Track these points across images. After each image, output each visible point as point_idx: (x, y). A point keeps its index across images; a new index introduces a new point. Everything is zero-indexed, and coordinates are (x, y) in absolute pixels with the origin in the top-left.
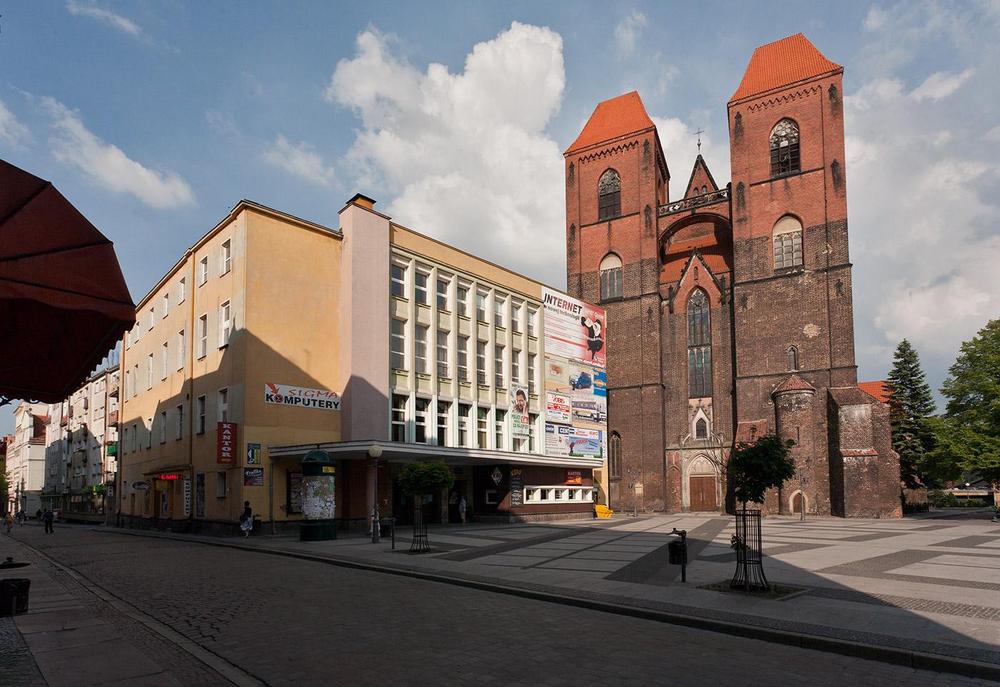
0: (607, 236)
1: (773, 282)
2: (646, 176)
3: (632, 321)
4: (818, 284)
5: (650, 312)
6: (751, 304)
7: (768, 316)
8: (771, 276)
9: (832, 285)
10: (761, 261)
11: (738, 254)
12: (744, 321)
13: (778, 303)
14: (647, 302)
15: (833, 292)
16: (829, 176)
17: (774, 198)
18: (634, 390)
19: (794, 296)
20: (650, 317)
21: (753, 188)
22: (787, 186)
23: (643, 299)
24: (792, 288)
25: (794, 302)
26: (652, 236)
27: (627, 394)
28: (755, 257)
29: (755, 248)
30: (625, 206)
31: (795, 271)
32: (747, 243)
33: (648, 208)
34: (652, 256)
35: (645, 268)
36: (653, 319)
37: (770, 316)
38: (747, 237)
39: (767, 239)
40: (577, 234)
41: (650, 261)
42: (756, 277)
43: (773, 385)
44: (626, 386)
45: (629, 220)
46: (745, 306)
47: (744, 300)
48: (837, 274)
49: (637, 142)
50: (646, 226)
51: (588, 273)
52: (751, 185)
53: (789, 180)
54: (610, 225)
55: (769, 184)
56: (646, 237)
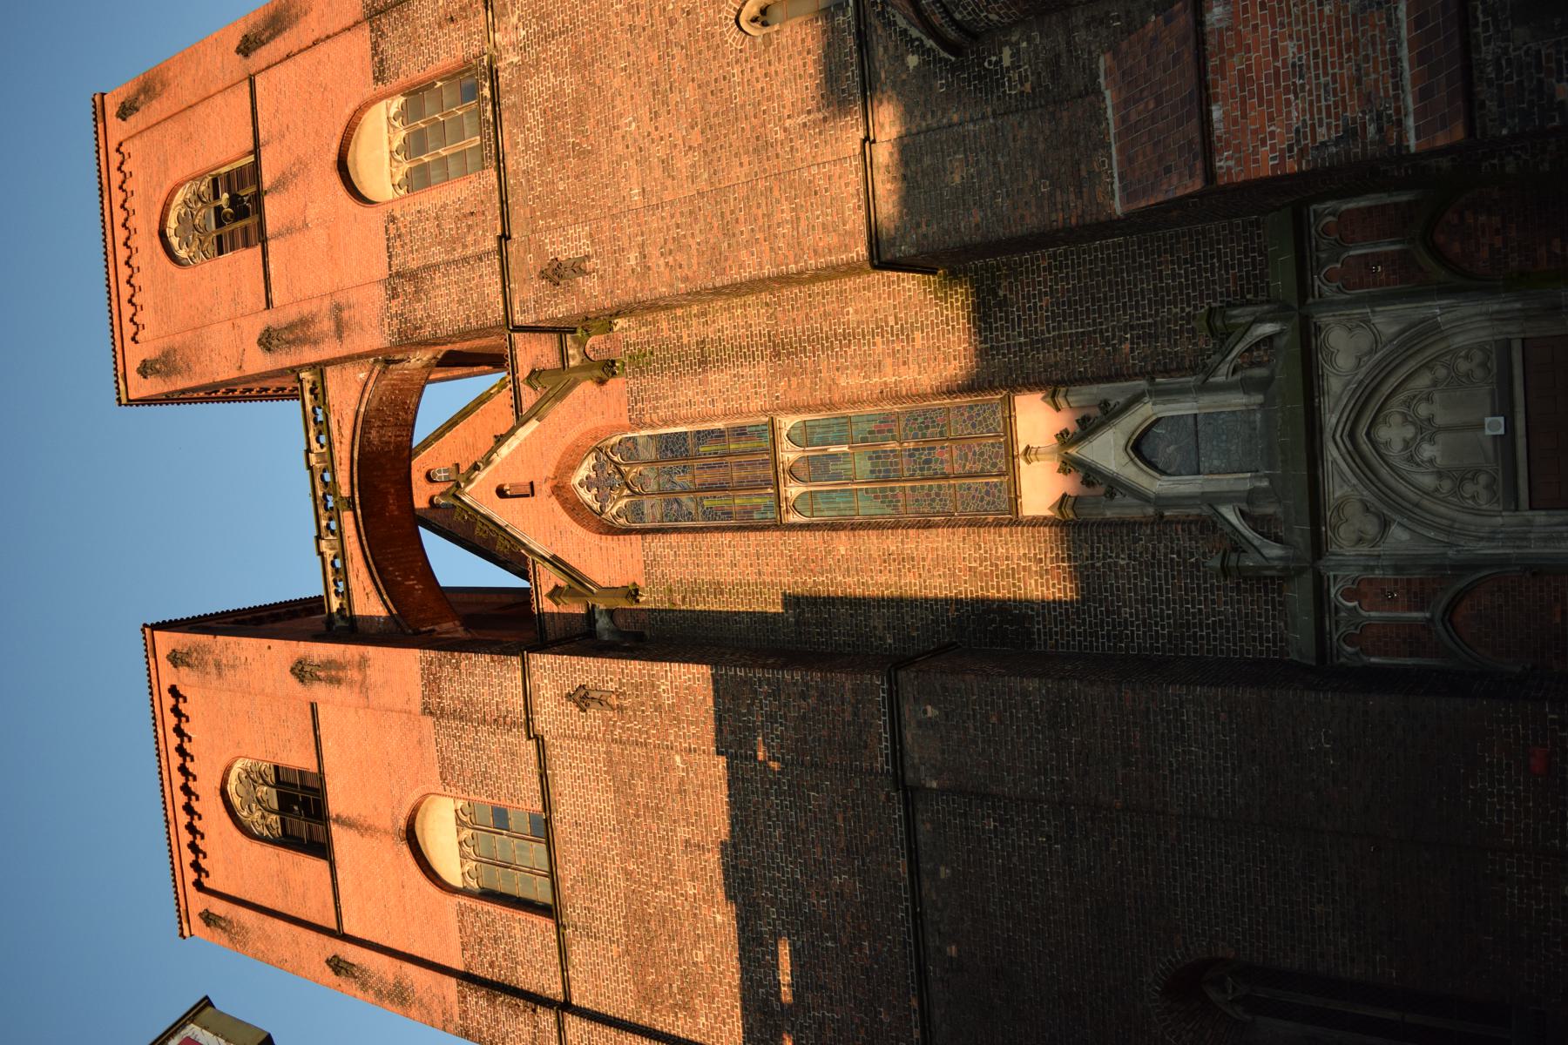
0: (366, 839)
1: (510, 162)
2: (233, 667)
3: (622, 788)
5: (582, 698)
10: (449, 225)
12: (633, 258)
14: (551, 713)
17: (299, 224)
18: (924, 828)
23: (541, 723)
24: (534, 86)
26: (363, 663)
27: (944, 872)
33: (301, 671)
34: (417, 667)
36: (612, 686)
37: (620, 148)
38: (379, 293)
39: (393, 219)
40: (352, 953)
41: (432, 682)
43: (912, 61)
44: (903, 869)
46: (578, 268)
47: (557, 274)
49: (173, 691)
50: (339, 681)
52: (269, 303)
54: (338, 820)
55: (272, 246)
56: (364, 688)
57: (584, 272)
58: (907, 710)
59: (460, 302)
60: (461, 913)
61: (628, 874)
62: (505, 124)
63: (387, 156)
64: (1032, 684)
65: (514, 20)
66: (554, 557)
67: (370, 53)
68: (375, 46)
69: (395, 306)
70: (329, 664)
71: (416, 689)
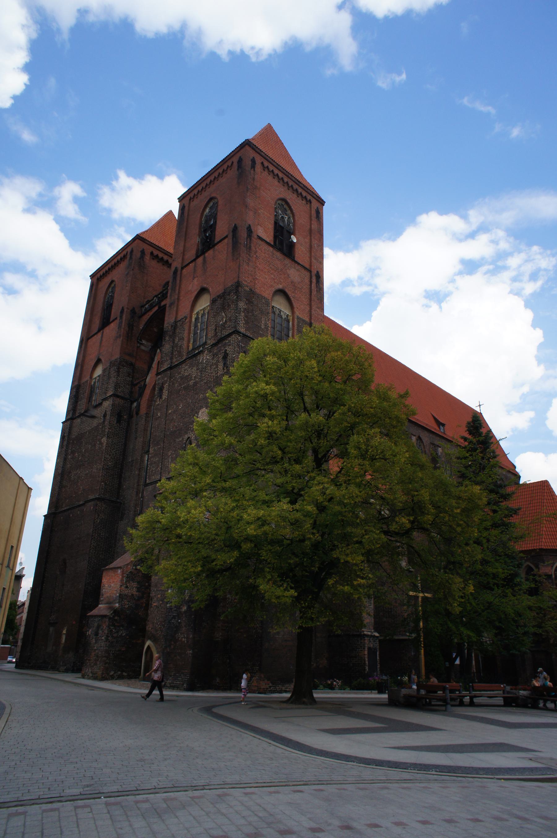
1: (183, 365)
4: (213, 358)
6: (165, 395)
7: (176, 405)
8: (184, 358)
9: (221, 356)
11: (165, 340)
13: (185, 388)
14: (106, 404)
15: (221, 366)
16: (231, 241)
17: (195, 276)
19: (195, 377)
20: (104, 421)
21: (184, 270)
22: (205, 261)
25: (195, 384)
28: (177, 340)
29: (178, 331)
30: (115, 311)
31: (201, 349)
32: (172, 326)
33: (122, 312)
35: (112, 369)
38: (172, 320)
39: (186, 320)
42: (175, 362)
45: (112, 324)
46: (161, 397)
48: (225, 344)
50: (119, 328)
51: (83, 383)
52: (182, 268)
53: (207, 255)
57: (160, 399)
58: (93, 503)
59: (165, 354)
60: (87, 382)
61: (86, 432)
62: (190, 360)
63: (202, 308)
64: (92, 530)
65: (208, 357)
66: (146, 385)
67: (218, 294)
68: (218, 296)
69: (170, 327)
70: (122, 322)
71: (113, 359)
